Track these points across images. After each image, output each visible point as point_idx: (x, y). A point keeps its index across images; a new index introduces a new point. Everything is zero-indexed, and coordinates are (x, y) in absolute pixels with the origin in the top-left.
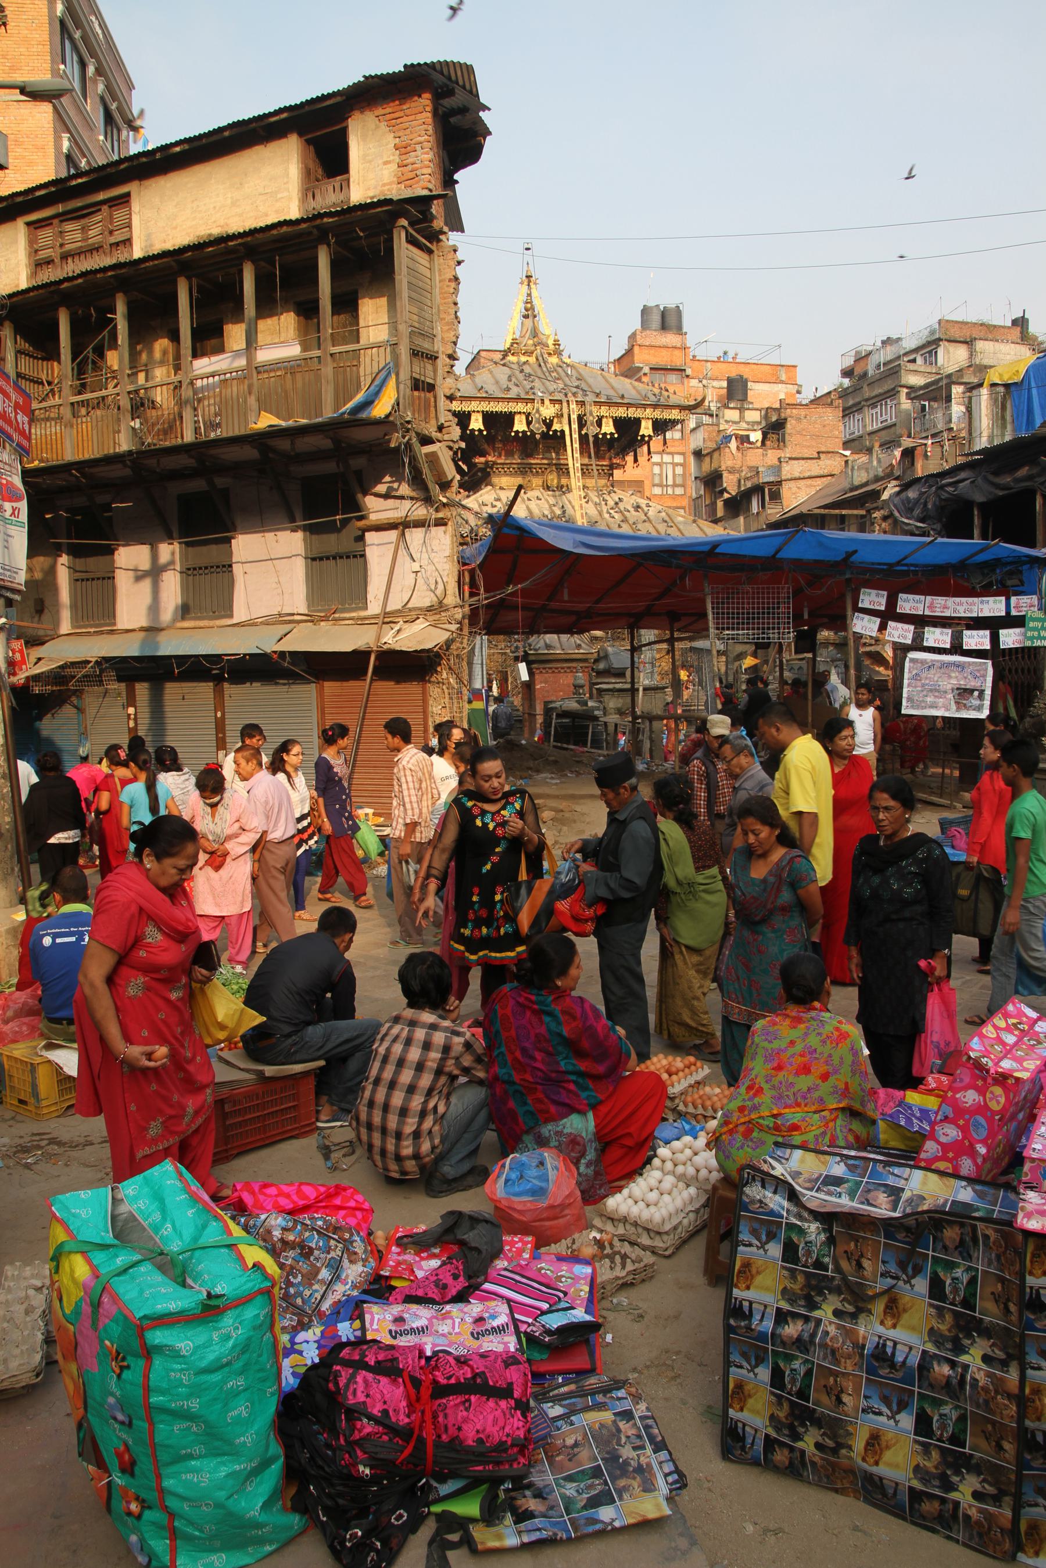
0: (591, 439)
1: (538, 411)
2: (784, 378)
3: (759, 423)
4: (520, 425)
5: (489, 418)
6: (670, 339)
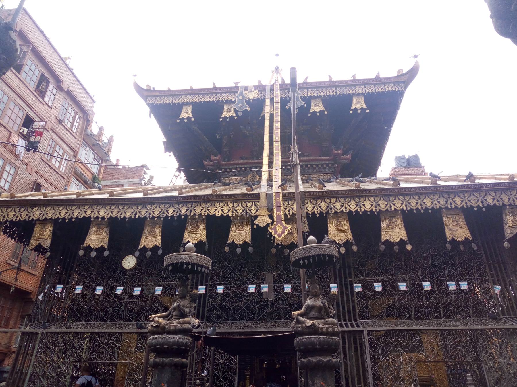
1: (241, 94)
5: (197, 107)
6: (414, 170)
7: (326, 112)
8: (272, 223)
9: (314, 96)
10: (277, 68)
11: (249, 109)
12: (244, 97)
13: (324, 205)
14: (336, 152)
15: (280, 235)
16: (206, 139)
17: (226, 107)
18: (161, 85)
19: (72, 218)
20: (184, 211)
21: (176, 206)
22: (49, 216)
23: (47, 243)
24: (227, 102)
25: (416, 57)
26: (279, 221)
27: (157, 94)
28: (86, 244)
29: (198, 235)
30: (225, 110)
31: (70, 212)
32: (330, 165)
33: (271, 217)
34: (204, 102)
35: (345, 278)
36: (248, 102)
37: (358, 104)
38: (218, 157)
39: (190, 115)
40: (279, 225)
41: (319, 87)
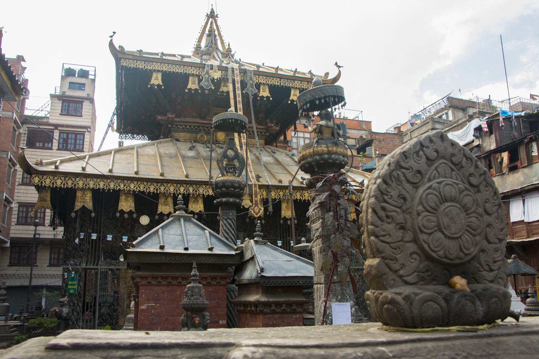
0: (251, 98)
1: (207, 73)
2: (364, 127)
3: (355, 146)
4: (192, 85)
7: (271, 99)
8: (252, 206)
9: (264, 83)
10: (212, 12)
11: (213, 88)
12: (209, 76)
13: (281, 193)
14: (270, 125)
15: (257, 214)
16: (162, 96)
17: (191, 79)
18: (131, 46)
19: (109, 189)
20: (191, 190)
21: (185, 186)
22: (91, 186)
23: (90, 205)
24: (193, 75)
25: (339, 67)
26: (256, 204)
27: (131, 57)
28: (119, 209)
29: (198, 206)
30: (190, 82)
31: (106, 184)
32: (263, 133)
33: (252, 202)
34: (173, 72)
35: (286, 237)
36: (213, 80)
37: (294, 96)
38: (173, 116)
39: (161, 83)
40: (257, 207)
41: (268, 76)
